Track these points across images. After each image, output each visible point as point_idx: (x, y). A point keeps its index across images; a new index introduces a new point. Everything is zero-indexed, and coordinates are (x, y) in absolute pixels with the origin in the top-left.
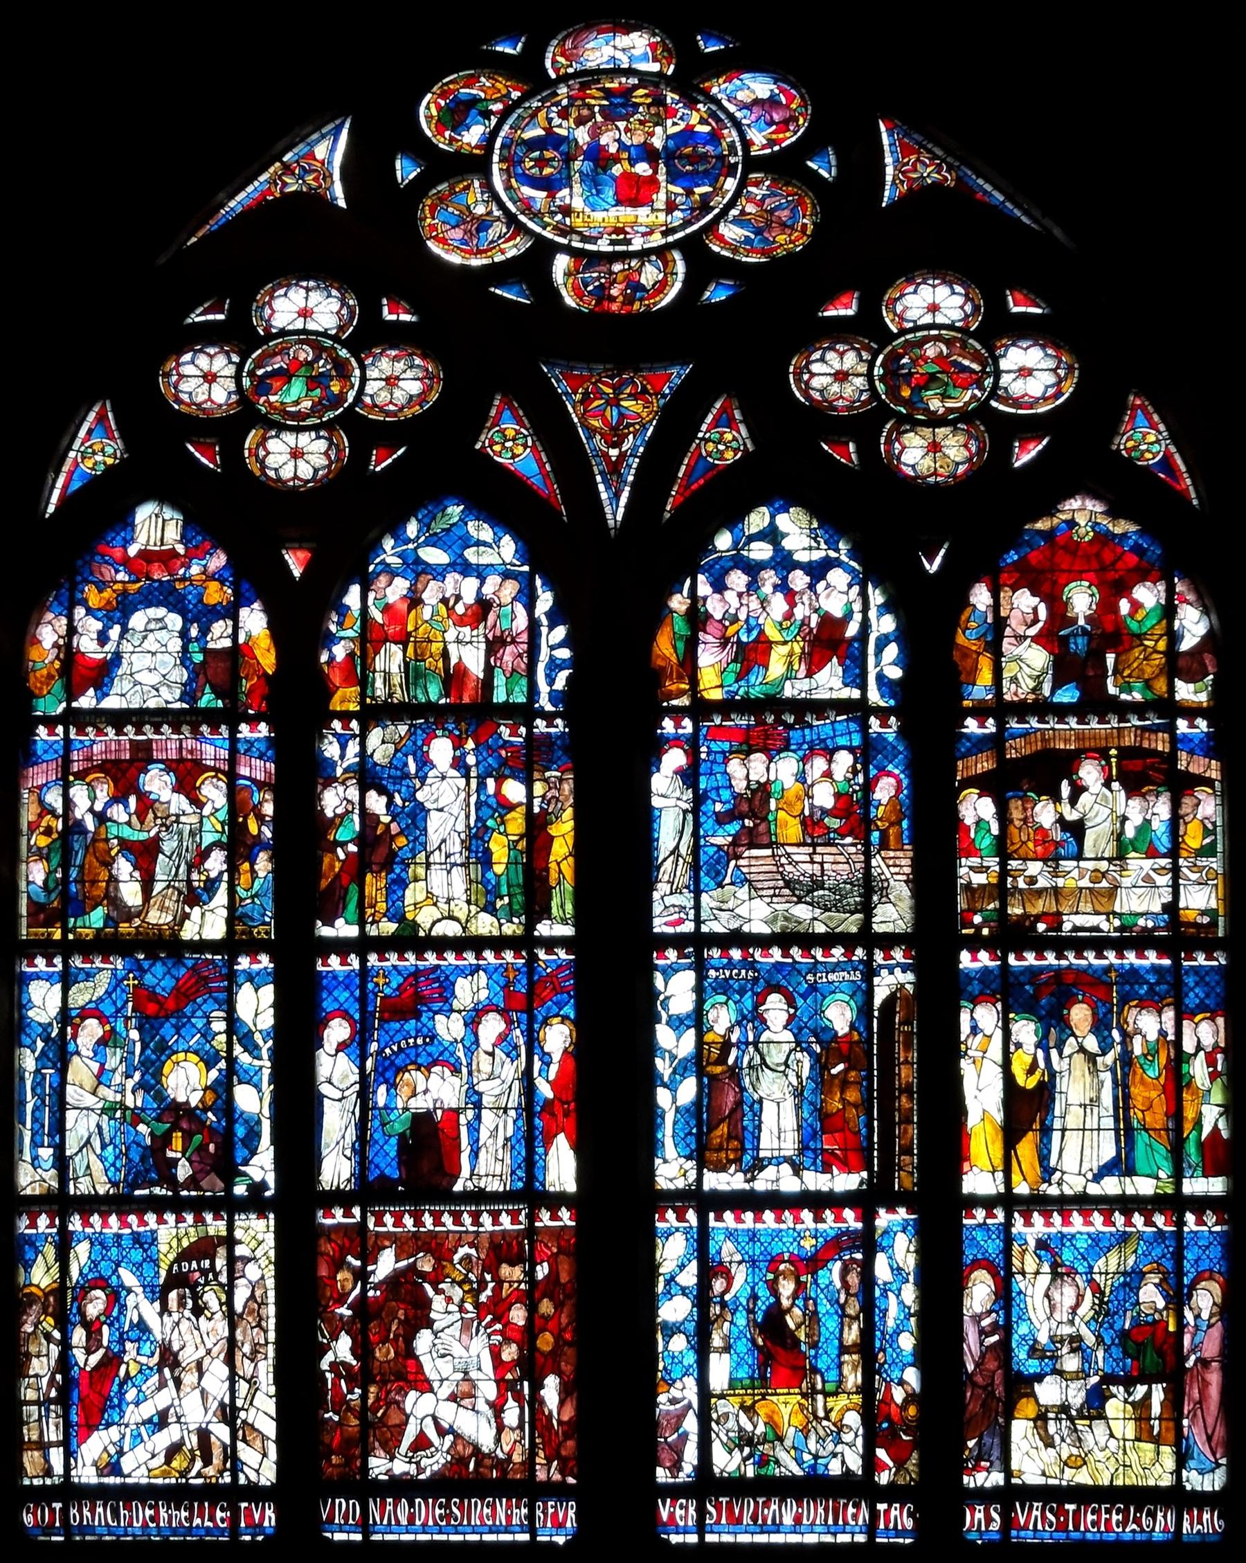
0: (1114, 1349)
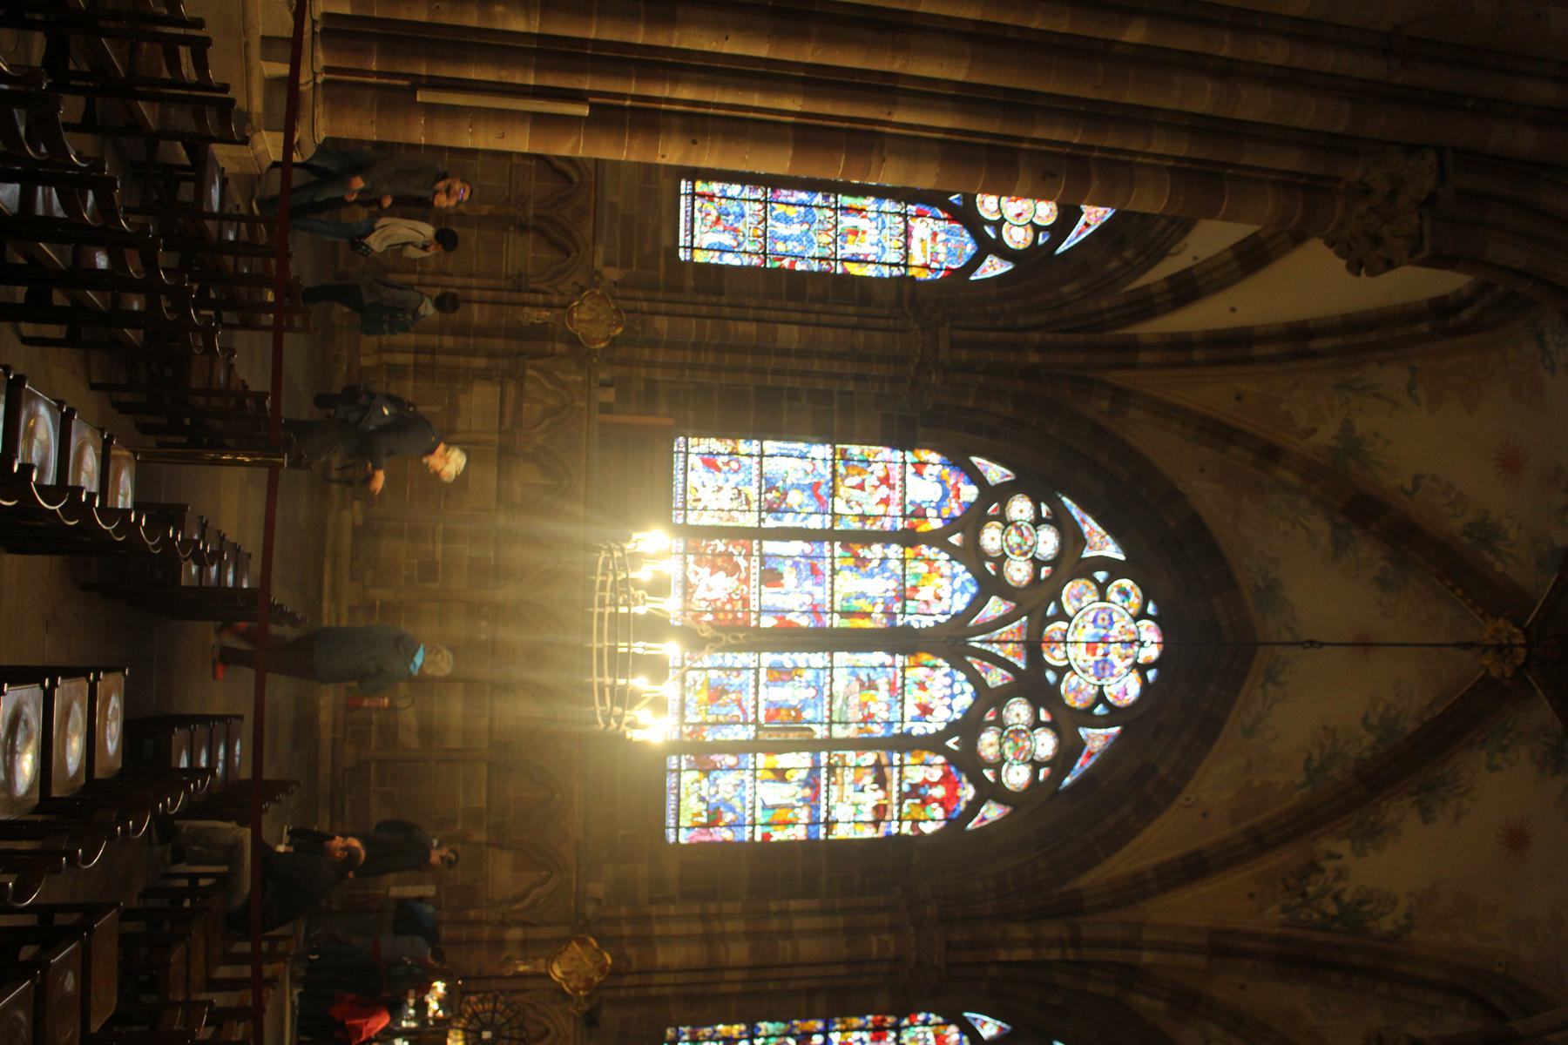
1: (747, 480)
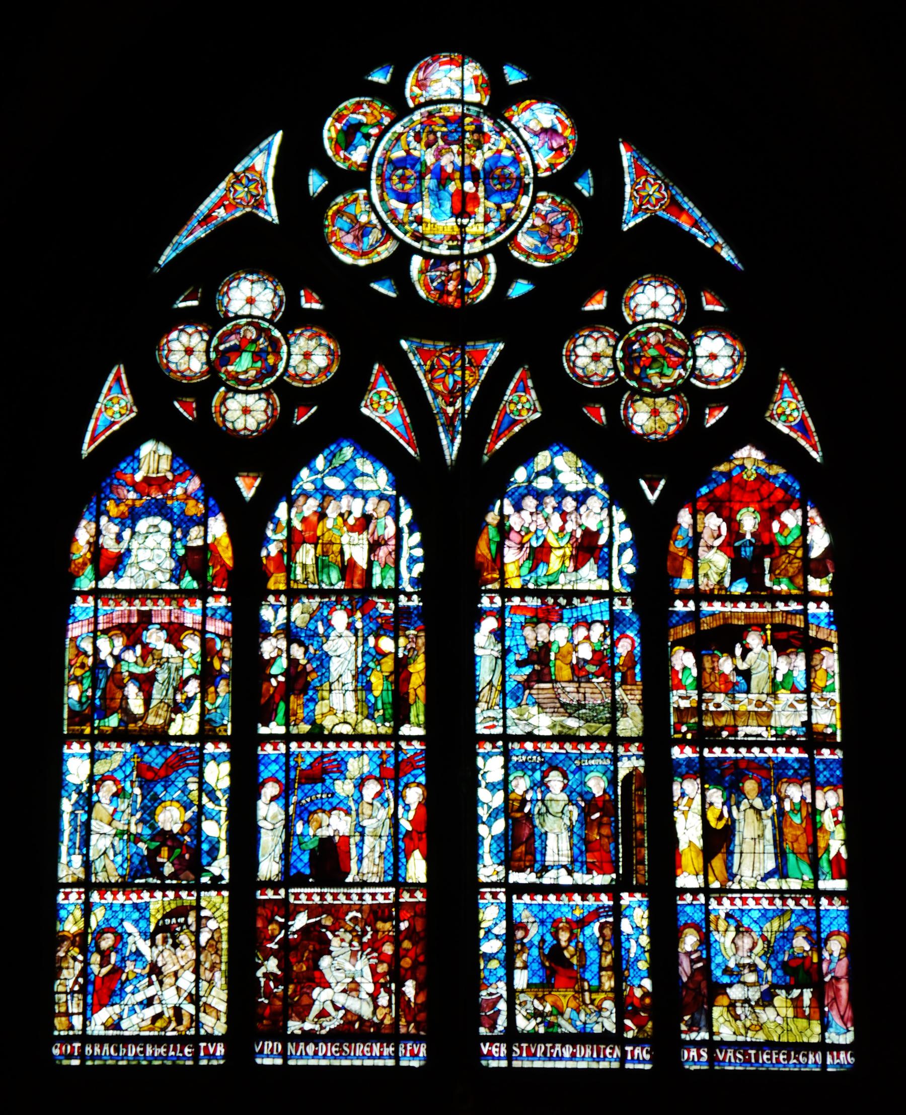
1: (136, 915)
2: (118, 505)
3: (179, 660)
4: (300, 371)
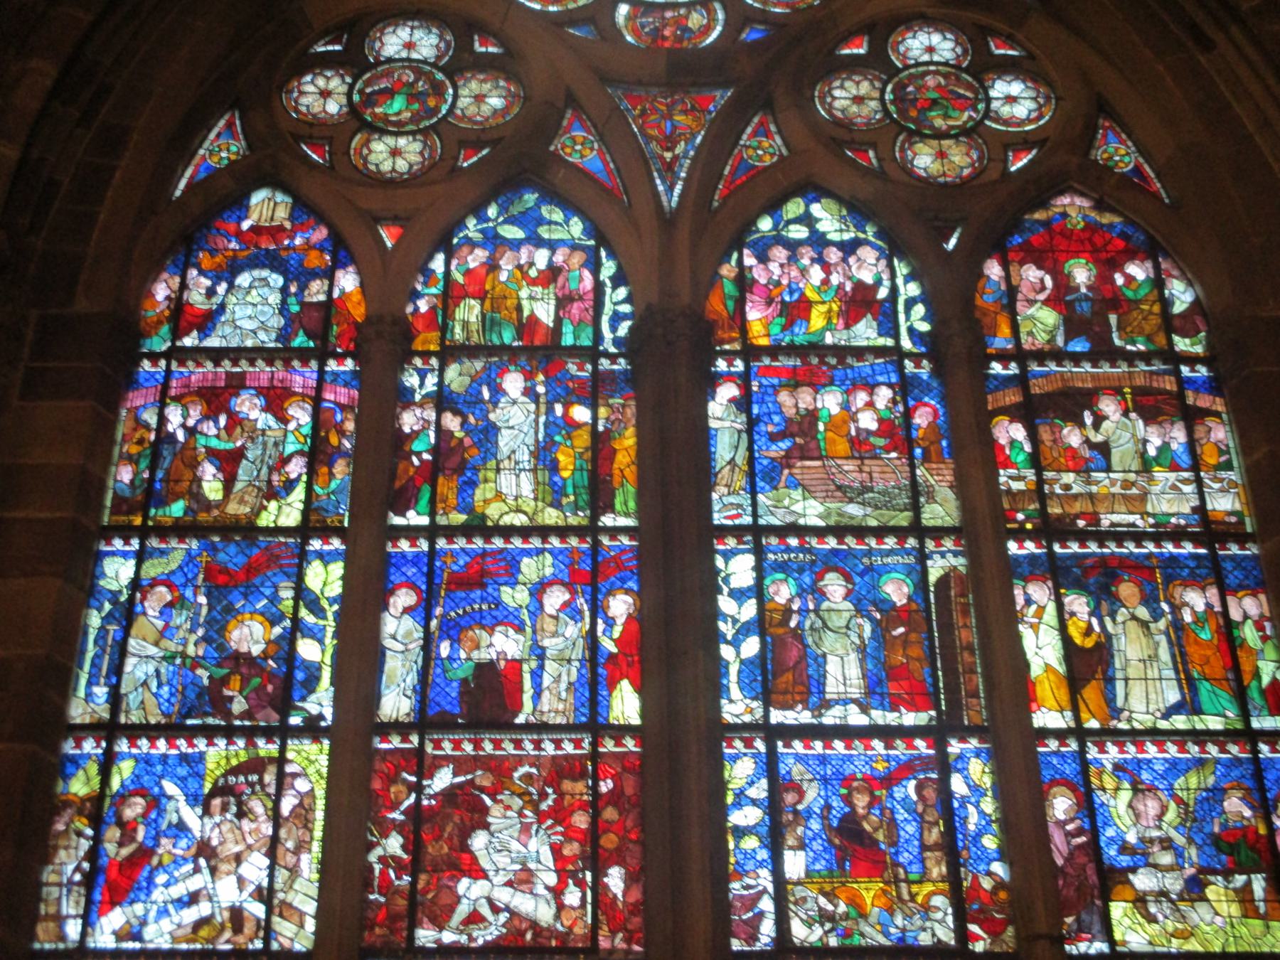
0: (1206, 848)
1: (182, 771)
2: (212, 256)
3: (279, 434)
4: (468, 113)
